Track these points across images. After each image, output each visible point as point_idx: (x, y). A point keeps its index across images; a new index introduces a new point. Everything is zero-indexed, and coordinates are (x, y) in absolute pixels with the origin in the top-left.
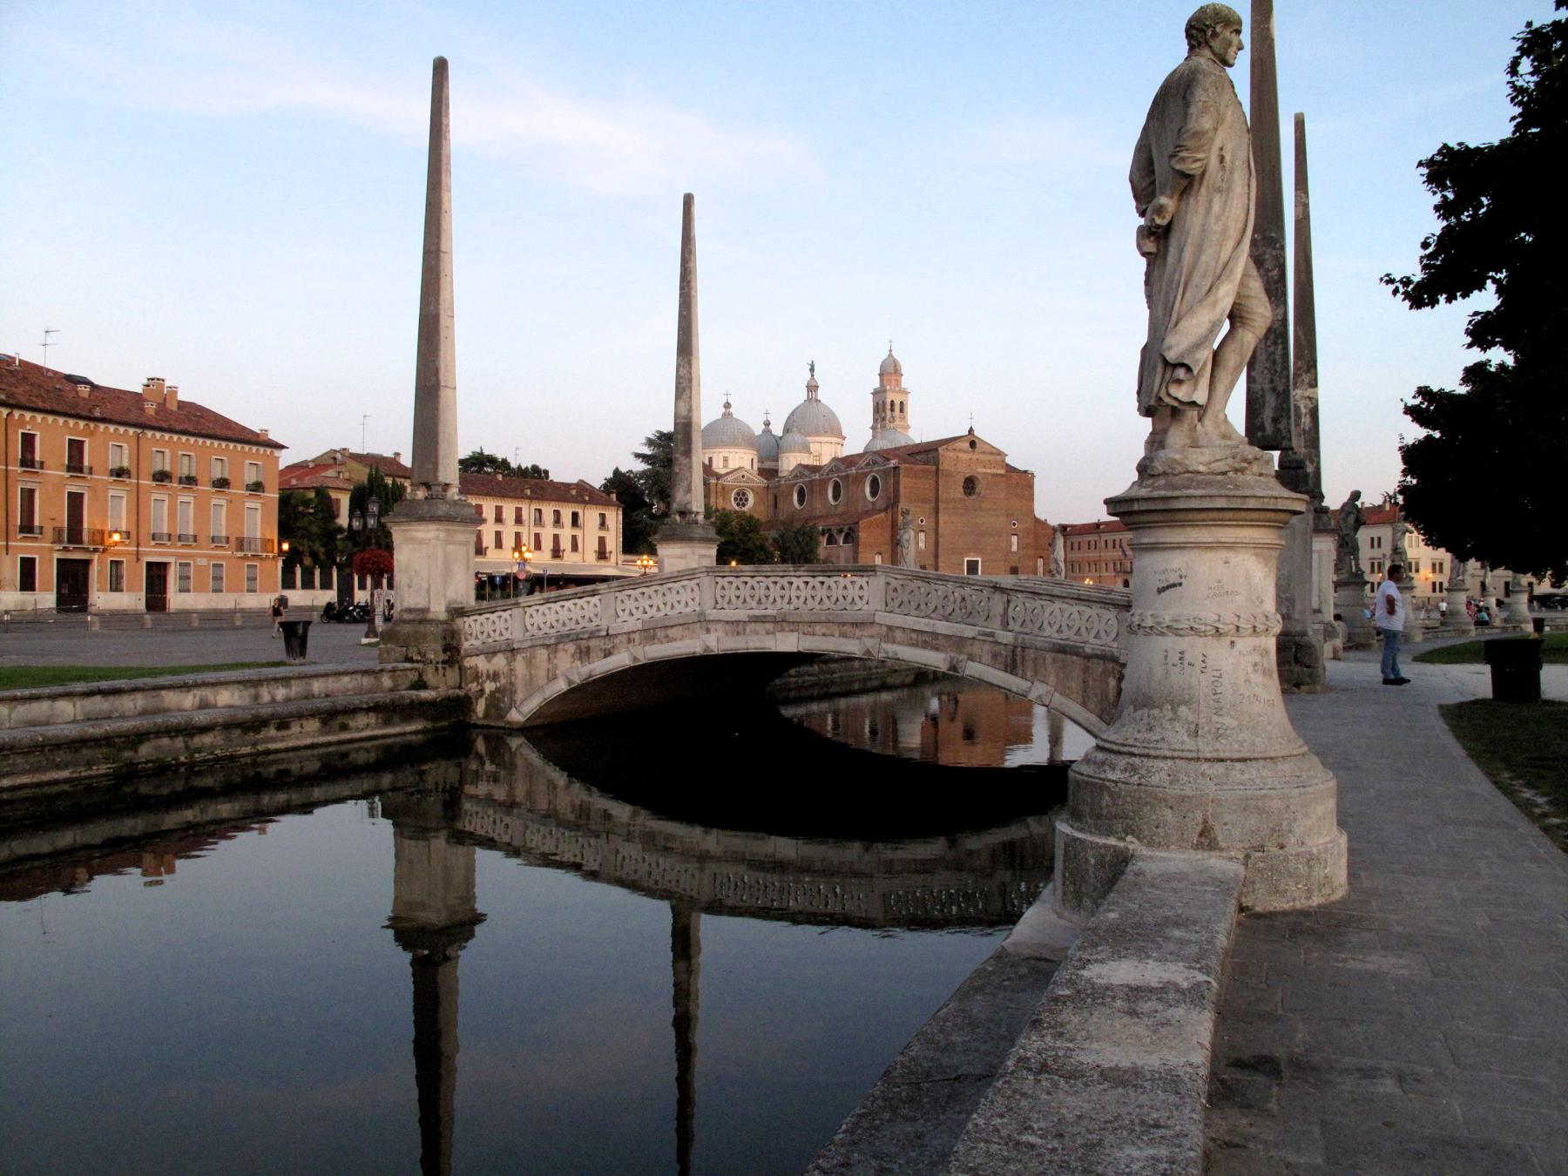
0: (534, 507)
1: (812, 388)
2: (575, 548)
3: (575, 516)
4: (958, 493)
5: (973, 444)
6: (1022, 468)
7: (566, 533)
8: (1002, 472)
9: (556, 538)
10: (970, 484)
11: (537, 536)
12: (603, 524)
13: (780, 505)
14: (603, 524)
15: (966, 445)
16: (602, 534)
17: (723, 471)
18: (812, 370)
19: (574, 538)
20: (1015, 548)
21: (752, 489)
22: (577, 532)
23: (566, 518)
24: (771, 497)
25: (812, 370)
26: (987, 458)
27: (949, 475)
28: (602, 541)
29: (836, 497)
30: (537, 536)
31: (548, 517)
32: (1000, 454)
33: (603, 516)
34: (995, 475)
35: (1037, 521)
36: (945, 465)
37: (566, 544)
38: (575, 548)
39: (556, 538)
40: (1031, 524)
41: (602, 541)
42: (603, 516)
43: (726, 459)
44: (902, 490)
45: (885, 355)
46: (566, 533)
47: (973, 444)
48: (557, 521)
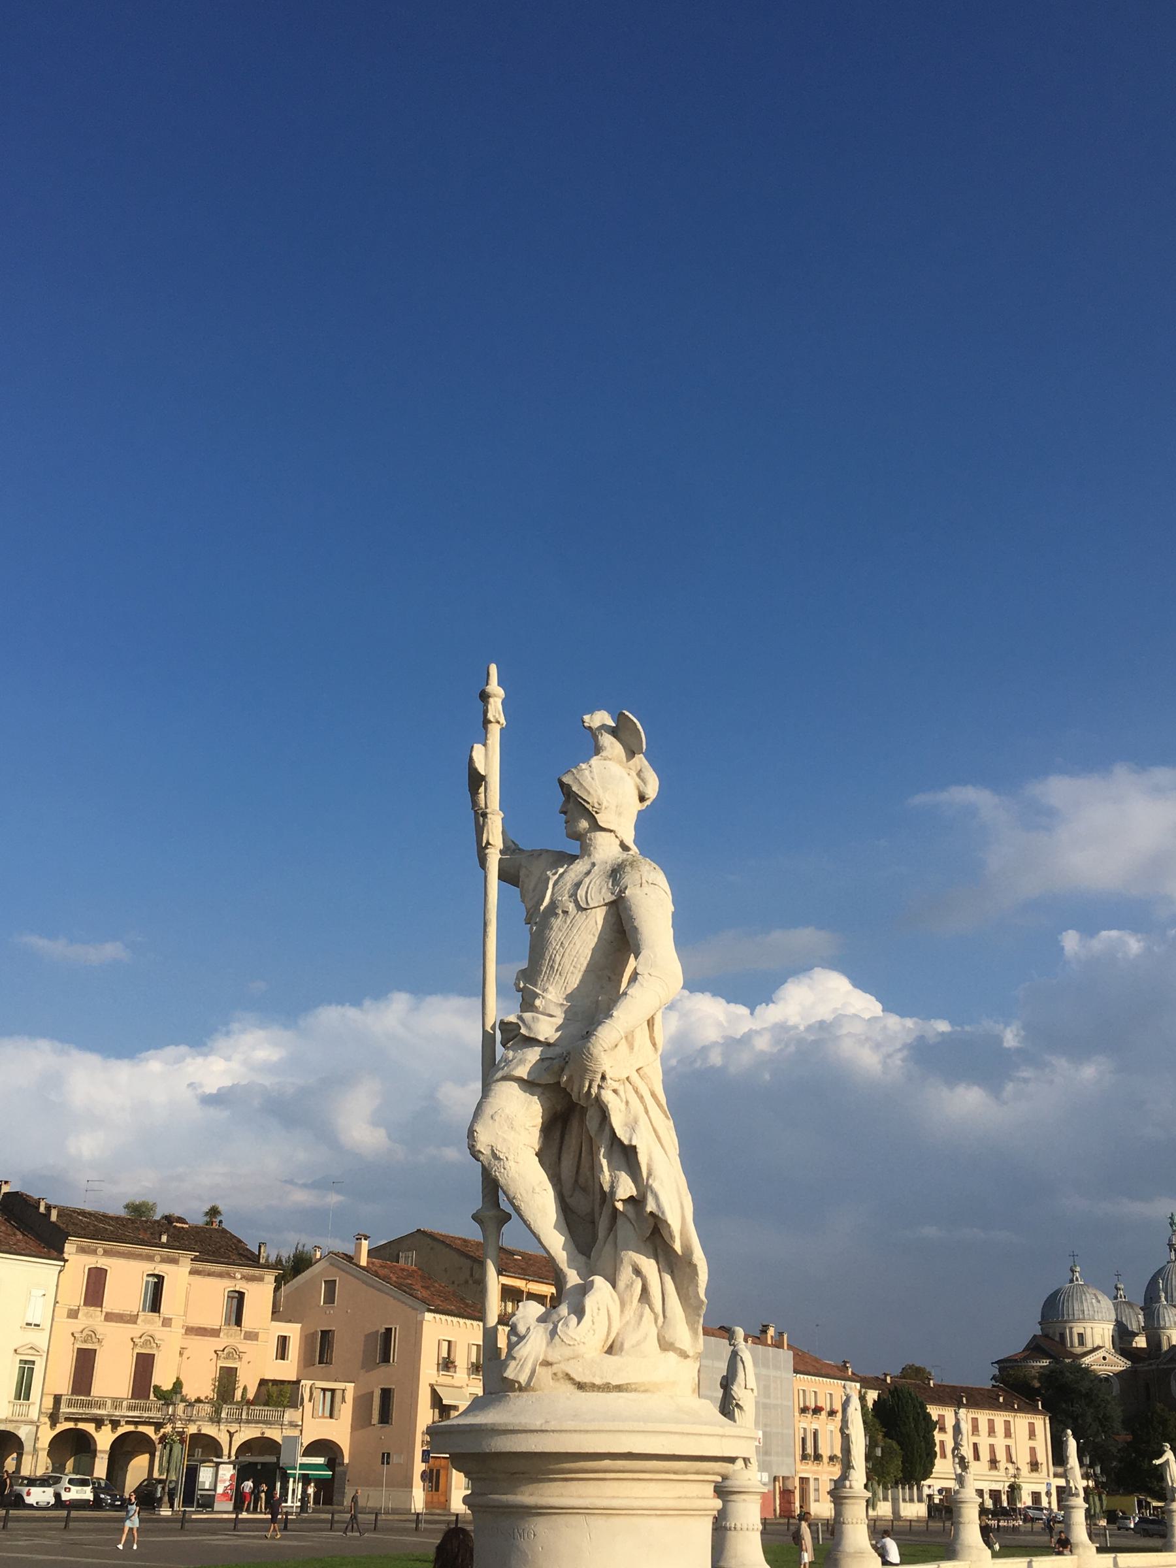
0: (971, 1415)
2: (1010, 1460)
3: (1007, 1423)
7: (1000, 1442)
9: (992, 1447)
11: (975, 1445)
12: (1032, 1434)
14: (1032, 1434)
16: (1032, 1443)
17: (1079, 1350)
19: (1008, 1448)
22: (1009, 1442)
23: (1000, 1428)
28: (1033, 1451)
30: (975, 1445)
31: (983, 1426)
33: (1032, 1425)
37: (1001, 1455)
38: (1010, 1460)
39: (992, 1447)
41: (1033, 1451)
42: (1032, 1425)
43: (1081, 1336)
46: (1000, 1442)
48: (992, 1431)
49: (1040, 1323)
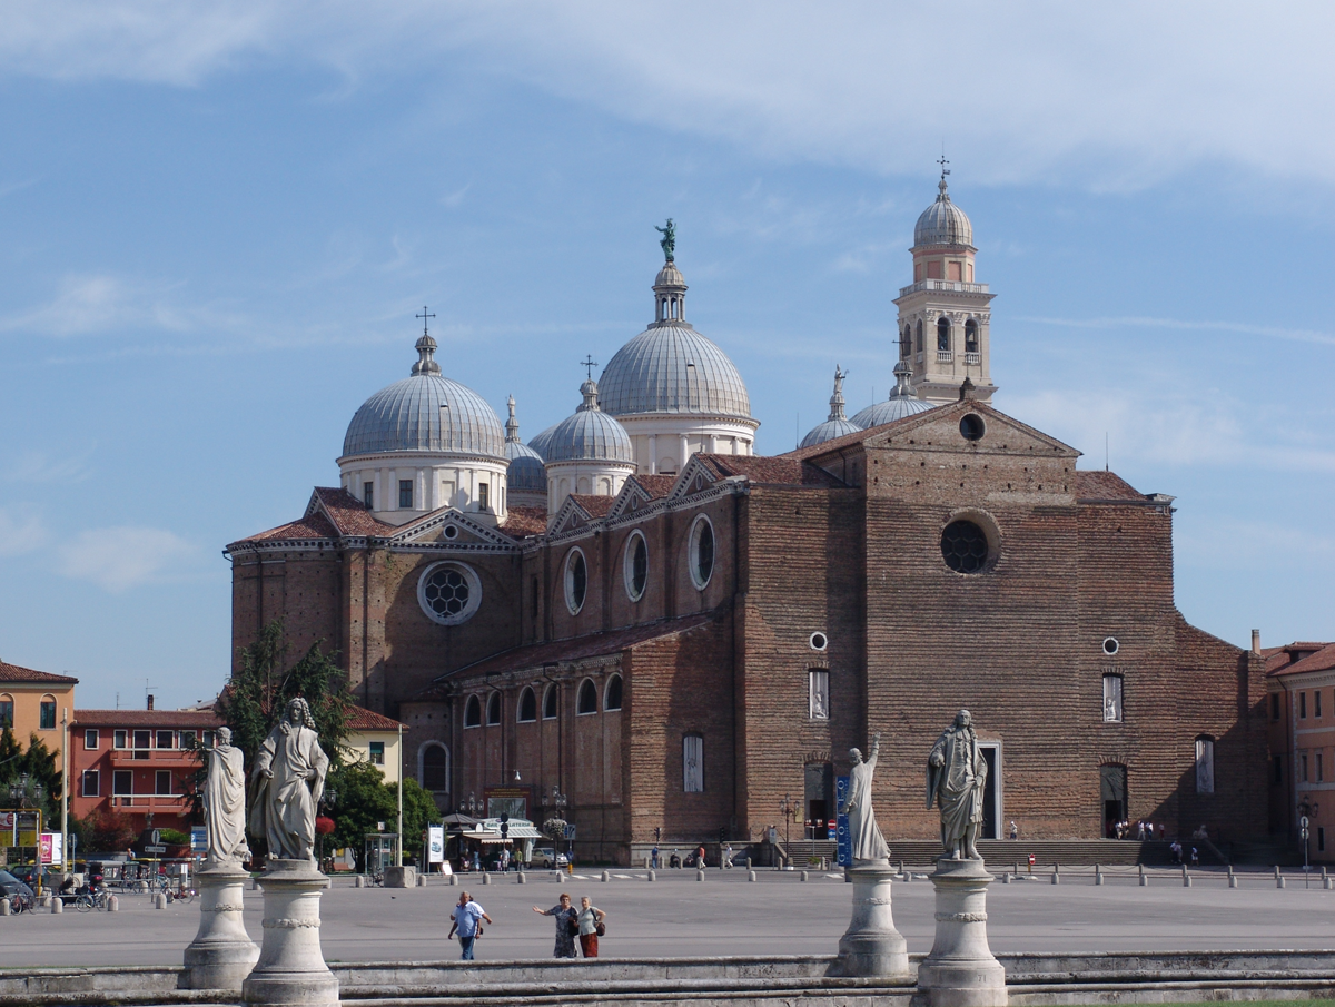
1: (667, 292)
4: (933, 563)
5: (972, 428)
6: (1144, 490)
8: (1066, 500)
10: (966, 543)
13: (541, 601)
15: (951, 430)
18: (668, 243)
20: (1112, 714)
21: (476, 564)
24: (527, 583)
25: (668, 243)
26: (1013, 463)
27: (898, 511)
29: (639, 581)
32: (1056, 449)
34: (1041, 511)
35: (1189, 637)
36: (883, 484)
40: (1161, 640)
43: (406, 489)
44: (753, 554)
45: (929, 201)
47: (972, 428)
49: (340, 462)
